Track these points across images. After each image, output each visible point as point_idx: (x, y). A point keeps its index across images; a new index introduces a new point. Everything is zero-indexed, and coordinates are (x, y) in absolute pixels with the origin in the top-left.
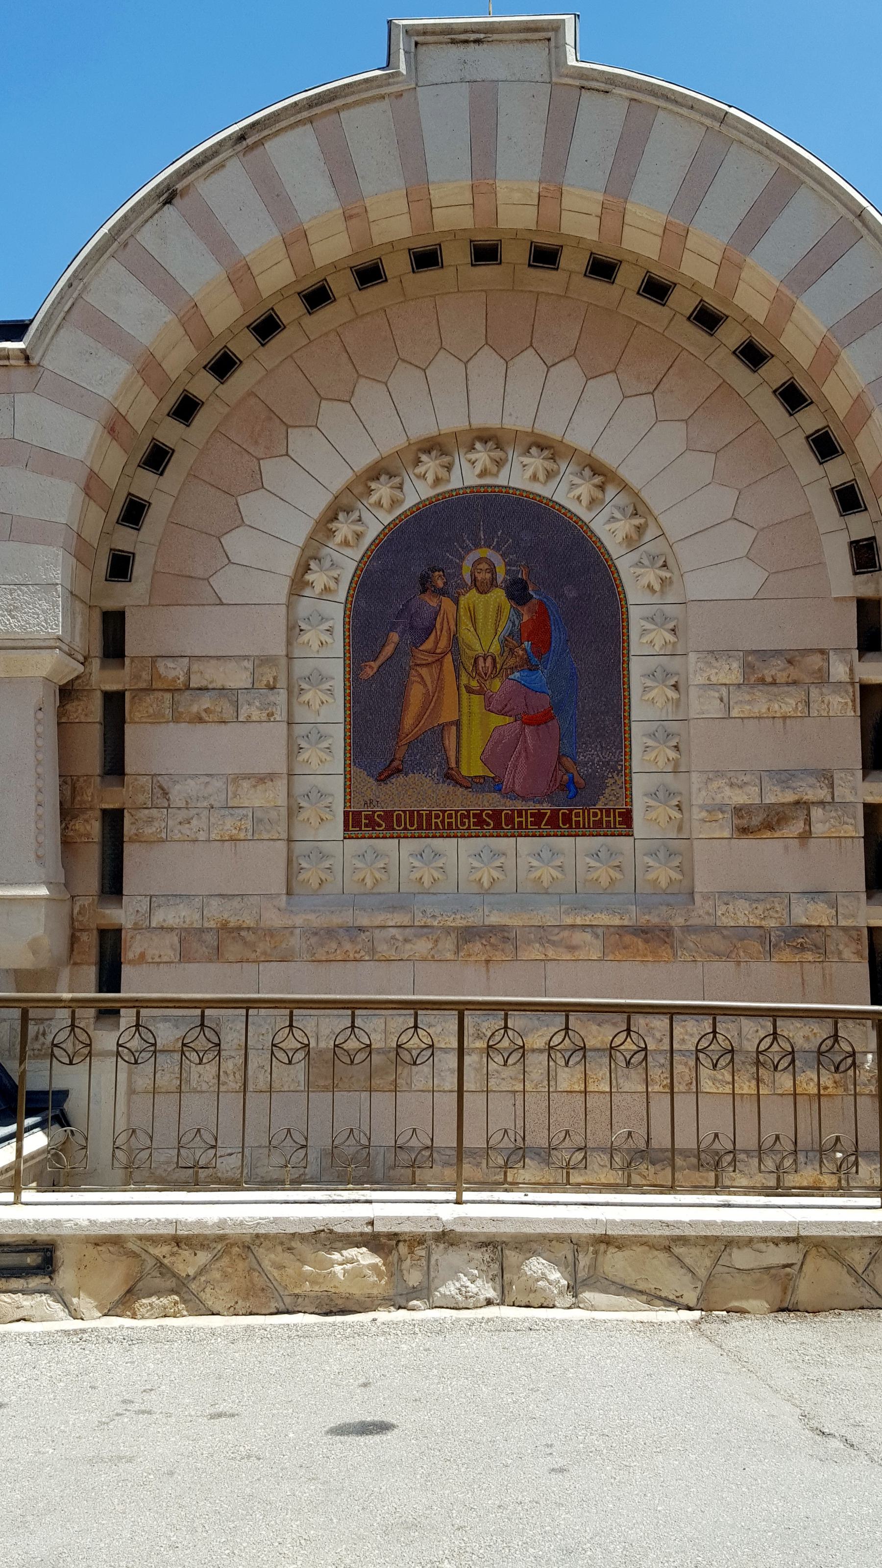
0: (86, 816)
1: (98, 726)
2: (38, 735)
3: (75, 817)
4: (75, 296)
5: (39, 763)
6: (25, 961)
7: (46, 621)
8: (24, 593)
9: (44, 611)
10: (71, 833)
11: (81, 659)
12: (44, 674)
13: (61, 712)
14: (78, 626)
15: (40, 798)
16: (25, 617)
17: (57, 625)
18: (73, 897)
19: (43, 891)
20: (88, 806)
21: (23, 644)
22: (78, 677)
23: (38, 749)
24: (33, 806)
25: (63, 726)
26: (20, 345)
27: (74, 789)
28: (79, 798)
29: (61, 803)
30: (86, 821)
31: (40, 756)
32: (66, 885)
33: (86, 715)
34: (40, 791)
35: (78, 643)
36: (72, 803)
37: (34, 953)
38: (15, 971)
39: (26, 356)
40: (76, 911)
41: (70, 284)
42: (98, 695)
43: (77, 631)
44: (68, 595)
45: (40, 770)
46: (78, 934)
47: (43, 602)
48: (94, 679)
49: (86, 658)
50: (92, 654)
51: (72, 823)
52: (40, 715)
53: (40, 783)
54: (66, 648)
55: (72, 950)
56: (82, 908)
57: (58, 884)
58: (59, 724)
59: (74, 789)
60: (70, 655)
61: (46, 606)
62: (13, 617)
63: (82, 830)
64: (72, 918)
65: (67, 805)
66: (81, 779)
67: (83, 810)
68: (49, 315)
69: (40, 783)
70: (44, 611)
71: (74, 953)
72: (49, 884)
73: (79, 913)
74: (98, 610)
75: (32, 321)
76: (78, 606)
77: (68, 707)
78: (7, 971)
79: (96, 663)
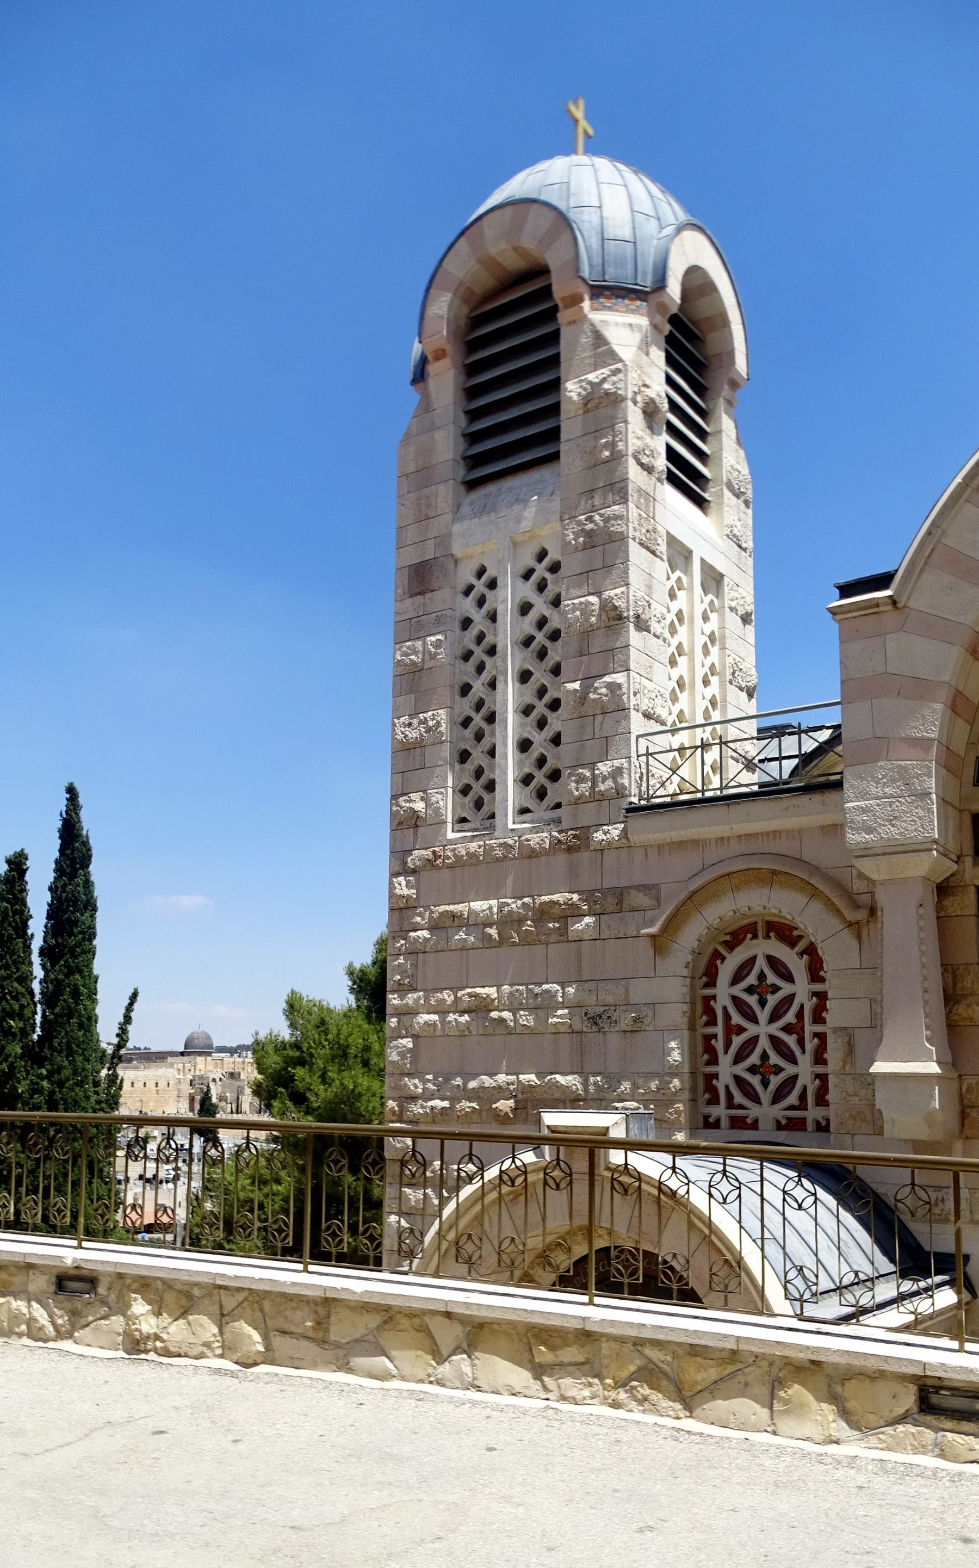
0: (968, 1002)
1: (974, 918)
2: (921, 929)
3: (957, 1002)
4: (934, 542)
5: (923, 953)
6: (923, 1133)
7: (922, 826)
8: (902, 804)
9: (920, 818)
10: (955, 1018)
11: (955, 858)
12: (923, 873)
13: (939, 907)
14: (951, 829)
15: (925, 986)
16: (904, 824)
17: (933, 829)
18: (960, 1076)
19: (933, 1068)
20: (969, 992)
21: (904, 848)
22: (952, 875)
23: (921, 942)
24: (920, 993)
25: (942, 921)
26: (888, 593)
27: (955, 977)
28: (959, 985)
29: (944, 990)
30: (968, 1006)
31: (923, 948)
32: (954, 1065)
33: (962, 909)
34: (925, 978)
35: (952, 845)
36: (954, 988)
37: (930, 1126)
38: (912, 1141)
39: (893, 601)
40: (964, 1088)
41: (929, 533)
42: (973, 889)
43: (950, 834)
44: (941, 802)
45: (924, 960)
46: (968, 1110)
47: (919, 810)
48: (967, 876)
49: (959, 857)
50: (965, 853)
51: (956, 1007)
52: (921, 911)
53: (925, 972)
54: (941, 849)
55: (963, 1125)
56: (970, 1086)
57: (946, 1063)
58: (938, 918)
59: (955, 977)
60: (945, 855)
61: (921, 813)
62: (893, 826)
63: (965, 1015)
64: (961, 1095)
65: (950, 991)
66: (961, 968)
67: (965, 996)
68: (912, 562)
69: (925, 972)
70: (920, 818)
71: (966, 1127)
72: (939, 1063)
73: (968, 1091)
74: (967, 813)
75: (897, 571)
76: (950, 810)
77: (946, 902)
78: (905, 1141)
79: (968, 861)
